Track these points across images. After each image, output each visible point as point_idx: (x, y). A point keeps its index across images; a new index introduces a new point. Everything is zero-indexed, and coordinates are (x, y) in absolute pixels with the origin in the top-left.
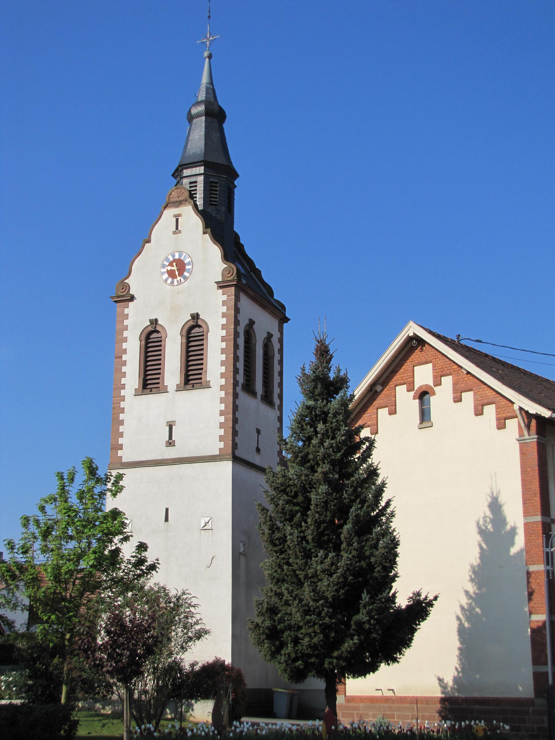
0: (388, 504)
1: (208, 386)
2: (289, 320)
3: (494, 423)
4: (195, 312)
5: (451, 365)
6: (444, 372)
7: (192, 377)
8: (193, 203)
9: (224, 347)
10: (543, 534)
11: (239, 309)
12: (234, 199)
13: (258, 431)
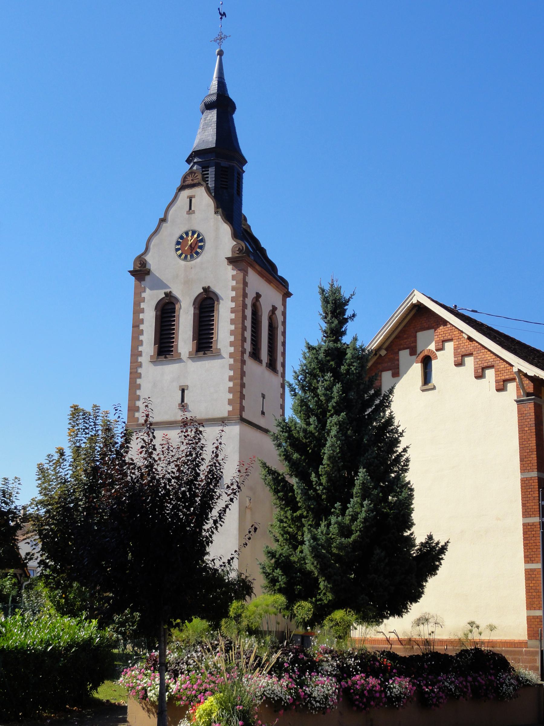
0: (405, 450)
1: (218, 355)
2: (292, 295)
3: (493, 385)
4: (206, 285)
5: (453, 330)
6: (446, 338)
7: (204, 343)
8: (205, 185)
9: (234, 317)
10: (539, 488)
11: (247, 283)
12: (242, 183)
13: (263, 396)
